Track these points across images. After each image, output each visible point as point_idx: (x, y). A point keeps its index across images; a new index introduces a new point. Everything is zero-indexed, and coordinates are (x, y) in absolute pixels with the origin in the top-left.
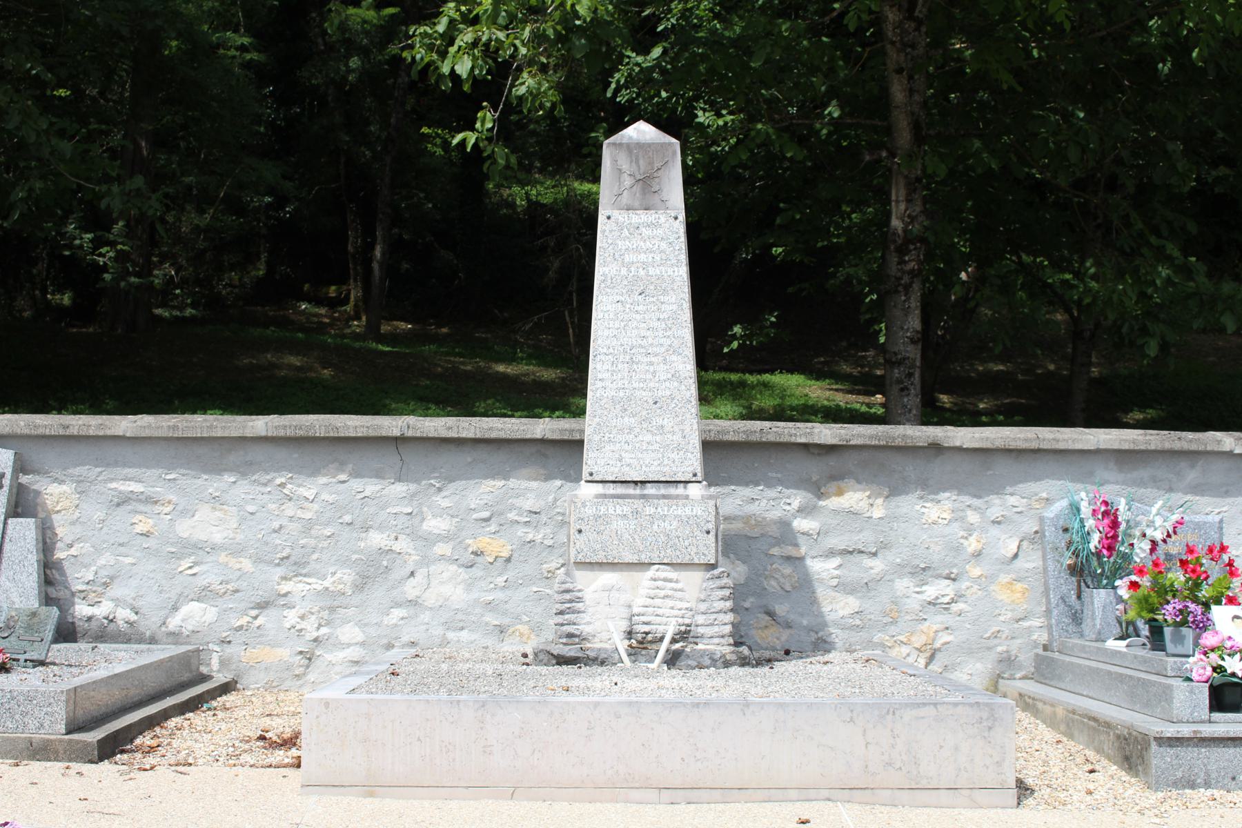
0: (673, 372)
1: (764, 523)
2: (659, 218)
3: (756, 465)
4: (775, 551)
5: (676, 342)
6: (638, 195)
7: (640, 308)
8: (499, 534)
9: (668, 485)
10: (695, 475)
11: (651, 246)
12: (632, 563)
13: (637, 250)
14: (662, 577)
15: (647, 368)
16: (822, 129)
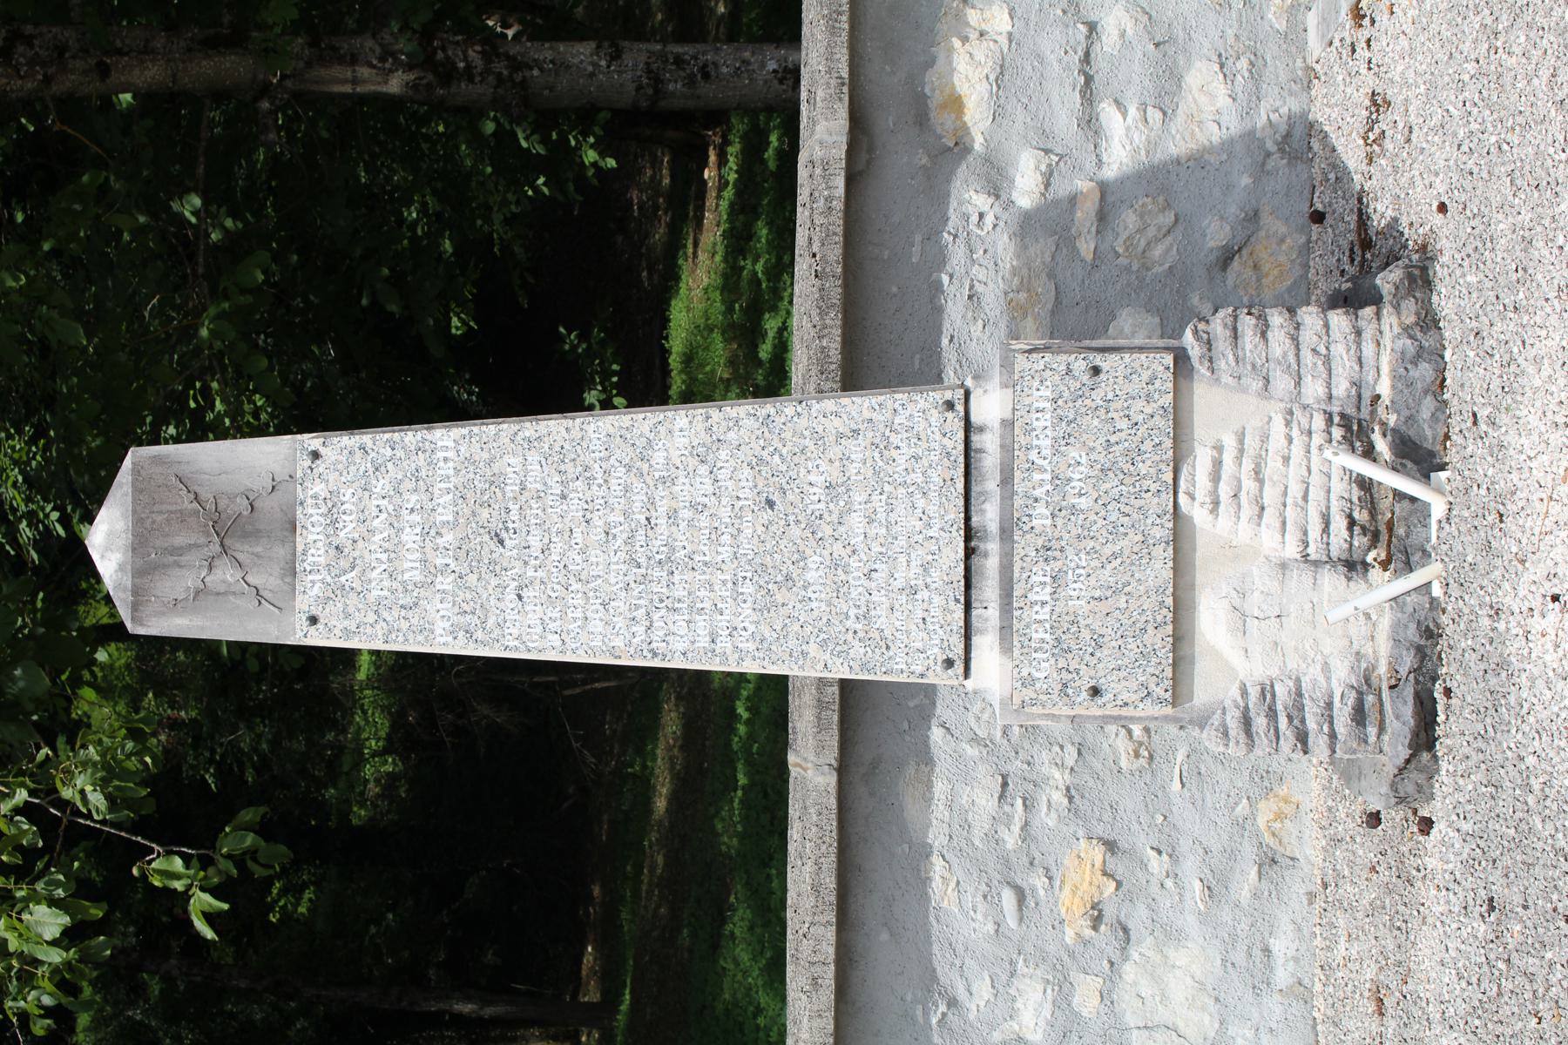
0: (693, 462)
1: (1025, 272)
2: (315, 497)
3: (894, 289)
4: (1086, 248)
5: (618, 454)
6: (259, 549)
7: (535, 542)
8: (1053, 868)
10: (950, 405)
11: (383, 516)
12: (1175, 560)
13: (393, 551)
14: (1209, 485)
15: (683, 525)
16: (224, 228)
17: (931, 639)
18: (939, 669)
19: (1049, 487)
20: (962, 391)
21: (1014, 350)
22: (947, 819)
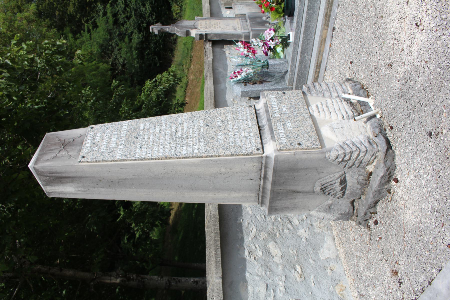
9: (258, 117)
22: (253, 296)
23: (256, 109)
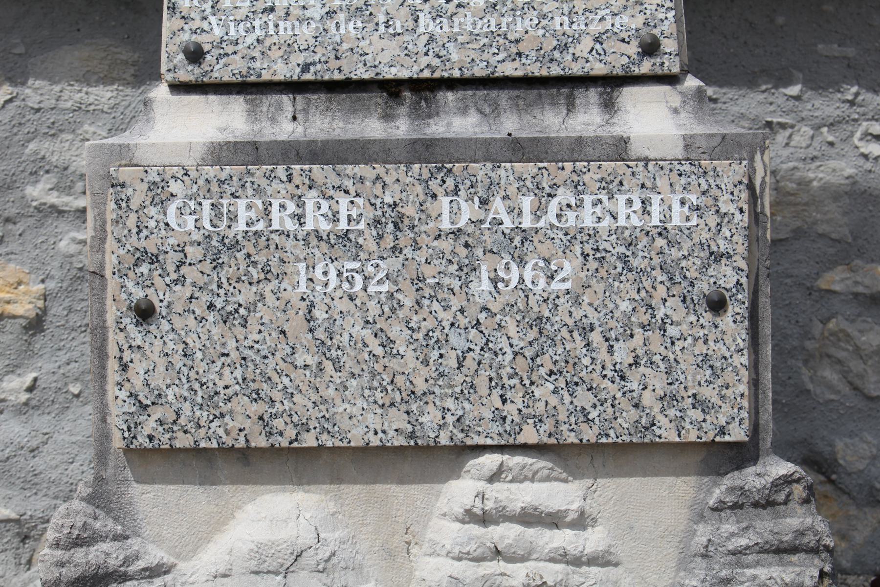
1: (804, 198)
3: (780, 20)
10: (651, 48)
12: (382, 449)
14: (516, 506)
17: (238, 22)
18: (185, 37)
19: (508, 224)
20: (676, 70)
21: (752, 160)
22: (62, 105)
23: (629, 95)
